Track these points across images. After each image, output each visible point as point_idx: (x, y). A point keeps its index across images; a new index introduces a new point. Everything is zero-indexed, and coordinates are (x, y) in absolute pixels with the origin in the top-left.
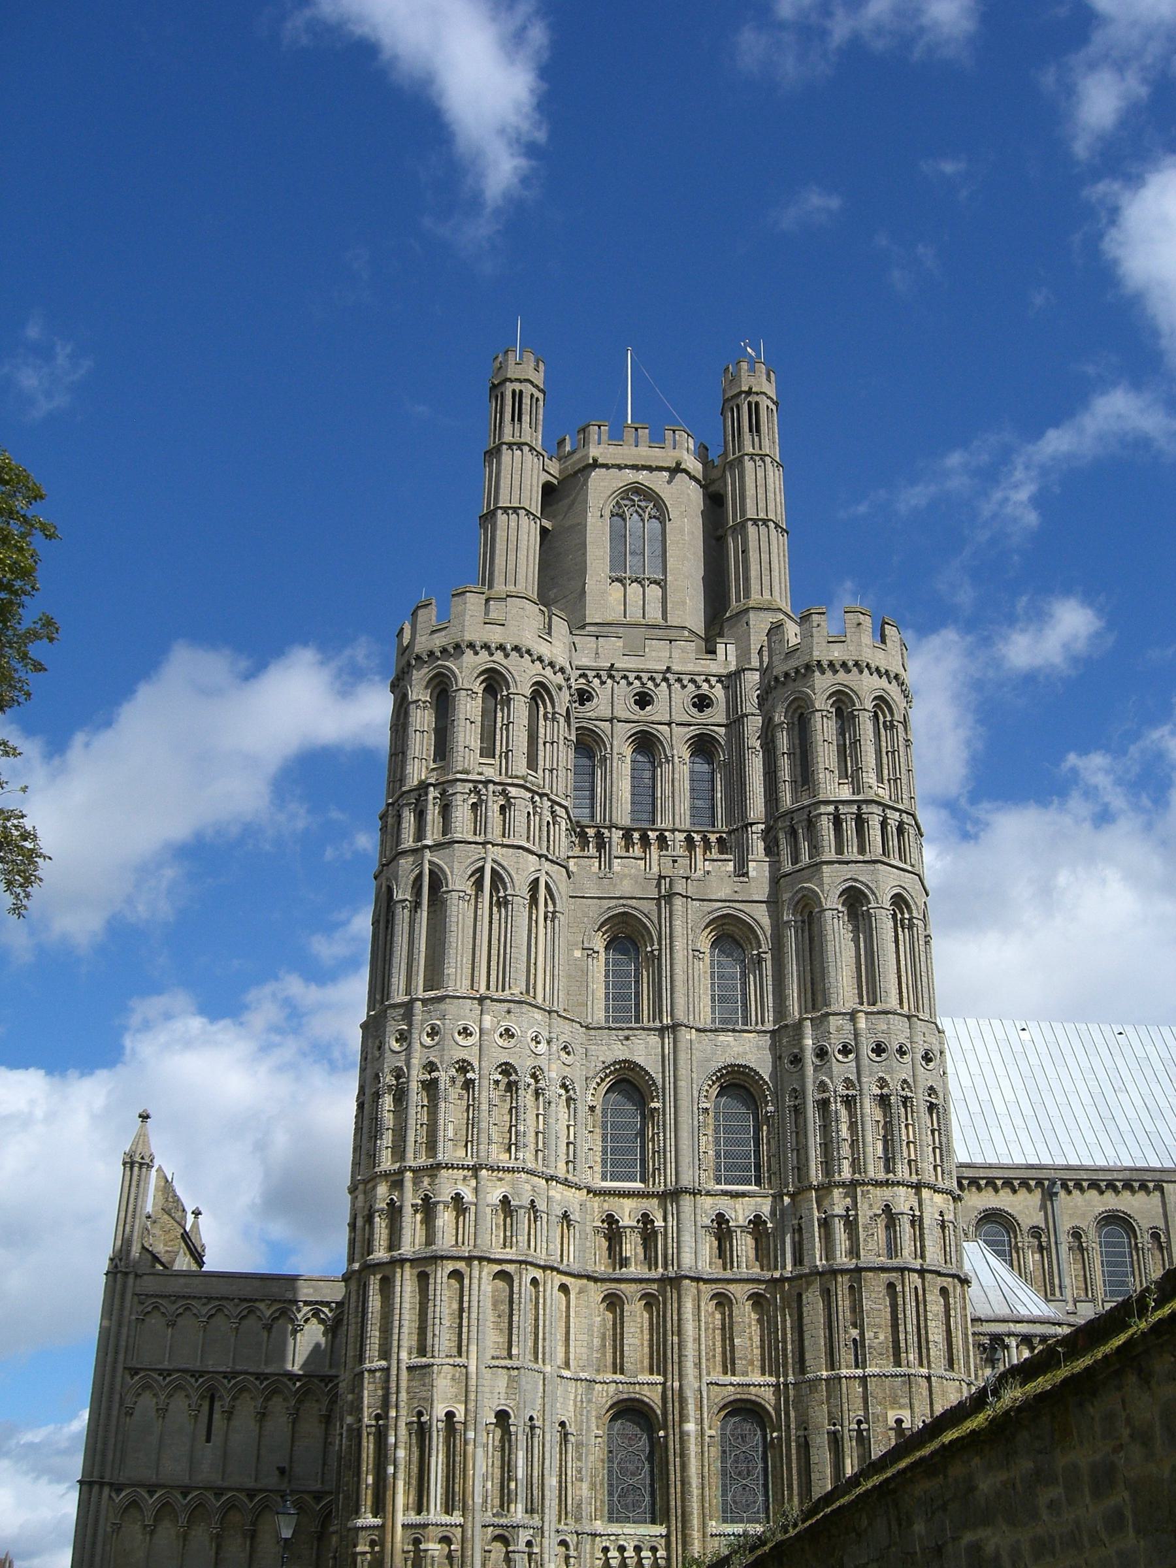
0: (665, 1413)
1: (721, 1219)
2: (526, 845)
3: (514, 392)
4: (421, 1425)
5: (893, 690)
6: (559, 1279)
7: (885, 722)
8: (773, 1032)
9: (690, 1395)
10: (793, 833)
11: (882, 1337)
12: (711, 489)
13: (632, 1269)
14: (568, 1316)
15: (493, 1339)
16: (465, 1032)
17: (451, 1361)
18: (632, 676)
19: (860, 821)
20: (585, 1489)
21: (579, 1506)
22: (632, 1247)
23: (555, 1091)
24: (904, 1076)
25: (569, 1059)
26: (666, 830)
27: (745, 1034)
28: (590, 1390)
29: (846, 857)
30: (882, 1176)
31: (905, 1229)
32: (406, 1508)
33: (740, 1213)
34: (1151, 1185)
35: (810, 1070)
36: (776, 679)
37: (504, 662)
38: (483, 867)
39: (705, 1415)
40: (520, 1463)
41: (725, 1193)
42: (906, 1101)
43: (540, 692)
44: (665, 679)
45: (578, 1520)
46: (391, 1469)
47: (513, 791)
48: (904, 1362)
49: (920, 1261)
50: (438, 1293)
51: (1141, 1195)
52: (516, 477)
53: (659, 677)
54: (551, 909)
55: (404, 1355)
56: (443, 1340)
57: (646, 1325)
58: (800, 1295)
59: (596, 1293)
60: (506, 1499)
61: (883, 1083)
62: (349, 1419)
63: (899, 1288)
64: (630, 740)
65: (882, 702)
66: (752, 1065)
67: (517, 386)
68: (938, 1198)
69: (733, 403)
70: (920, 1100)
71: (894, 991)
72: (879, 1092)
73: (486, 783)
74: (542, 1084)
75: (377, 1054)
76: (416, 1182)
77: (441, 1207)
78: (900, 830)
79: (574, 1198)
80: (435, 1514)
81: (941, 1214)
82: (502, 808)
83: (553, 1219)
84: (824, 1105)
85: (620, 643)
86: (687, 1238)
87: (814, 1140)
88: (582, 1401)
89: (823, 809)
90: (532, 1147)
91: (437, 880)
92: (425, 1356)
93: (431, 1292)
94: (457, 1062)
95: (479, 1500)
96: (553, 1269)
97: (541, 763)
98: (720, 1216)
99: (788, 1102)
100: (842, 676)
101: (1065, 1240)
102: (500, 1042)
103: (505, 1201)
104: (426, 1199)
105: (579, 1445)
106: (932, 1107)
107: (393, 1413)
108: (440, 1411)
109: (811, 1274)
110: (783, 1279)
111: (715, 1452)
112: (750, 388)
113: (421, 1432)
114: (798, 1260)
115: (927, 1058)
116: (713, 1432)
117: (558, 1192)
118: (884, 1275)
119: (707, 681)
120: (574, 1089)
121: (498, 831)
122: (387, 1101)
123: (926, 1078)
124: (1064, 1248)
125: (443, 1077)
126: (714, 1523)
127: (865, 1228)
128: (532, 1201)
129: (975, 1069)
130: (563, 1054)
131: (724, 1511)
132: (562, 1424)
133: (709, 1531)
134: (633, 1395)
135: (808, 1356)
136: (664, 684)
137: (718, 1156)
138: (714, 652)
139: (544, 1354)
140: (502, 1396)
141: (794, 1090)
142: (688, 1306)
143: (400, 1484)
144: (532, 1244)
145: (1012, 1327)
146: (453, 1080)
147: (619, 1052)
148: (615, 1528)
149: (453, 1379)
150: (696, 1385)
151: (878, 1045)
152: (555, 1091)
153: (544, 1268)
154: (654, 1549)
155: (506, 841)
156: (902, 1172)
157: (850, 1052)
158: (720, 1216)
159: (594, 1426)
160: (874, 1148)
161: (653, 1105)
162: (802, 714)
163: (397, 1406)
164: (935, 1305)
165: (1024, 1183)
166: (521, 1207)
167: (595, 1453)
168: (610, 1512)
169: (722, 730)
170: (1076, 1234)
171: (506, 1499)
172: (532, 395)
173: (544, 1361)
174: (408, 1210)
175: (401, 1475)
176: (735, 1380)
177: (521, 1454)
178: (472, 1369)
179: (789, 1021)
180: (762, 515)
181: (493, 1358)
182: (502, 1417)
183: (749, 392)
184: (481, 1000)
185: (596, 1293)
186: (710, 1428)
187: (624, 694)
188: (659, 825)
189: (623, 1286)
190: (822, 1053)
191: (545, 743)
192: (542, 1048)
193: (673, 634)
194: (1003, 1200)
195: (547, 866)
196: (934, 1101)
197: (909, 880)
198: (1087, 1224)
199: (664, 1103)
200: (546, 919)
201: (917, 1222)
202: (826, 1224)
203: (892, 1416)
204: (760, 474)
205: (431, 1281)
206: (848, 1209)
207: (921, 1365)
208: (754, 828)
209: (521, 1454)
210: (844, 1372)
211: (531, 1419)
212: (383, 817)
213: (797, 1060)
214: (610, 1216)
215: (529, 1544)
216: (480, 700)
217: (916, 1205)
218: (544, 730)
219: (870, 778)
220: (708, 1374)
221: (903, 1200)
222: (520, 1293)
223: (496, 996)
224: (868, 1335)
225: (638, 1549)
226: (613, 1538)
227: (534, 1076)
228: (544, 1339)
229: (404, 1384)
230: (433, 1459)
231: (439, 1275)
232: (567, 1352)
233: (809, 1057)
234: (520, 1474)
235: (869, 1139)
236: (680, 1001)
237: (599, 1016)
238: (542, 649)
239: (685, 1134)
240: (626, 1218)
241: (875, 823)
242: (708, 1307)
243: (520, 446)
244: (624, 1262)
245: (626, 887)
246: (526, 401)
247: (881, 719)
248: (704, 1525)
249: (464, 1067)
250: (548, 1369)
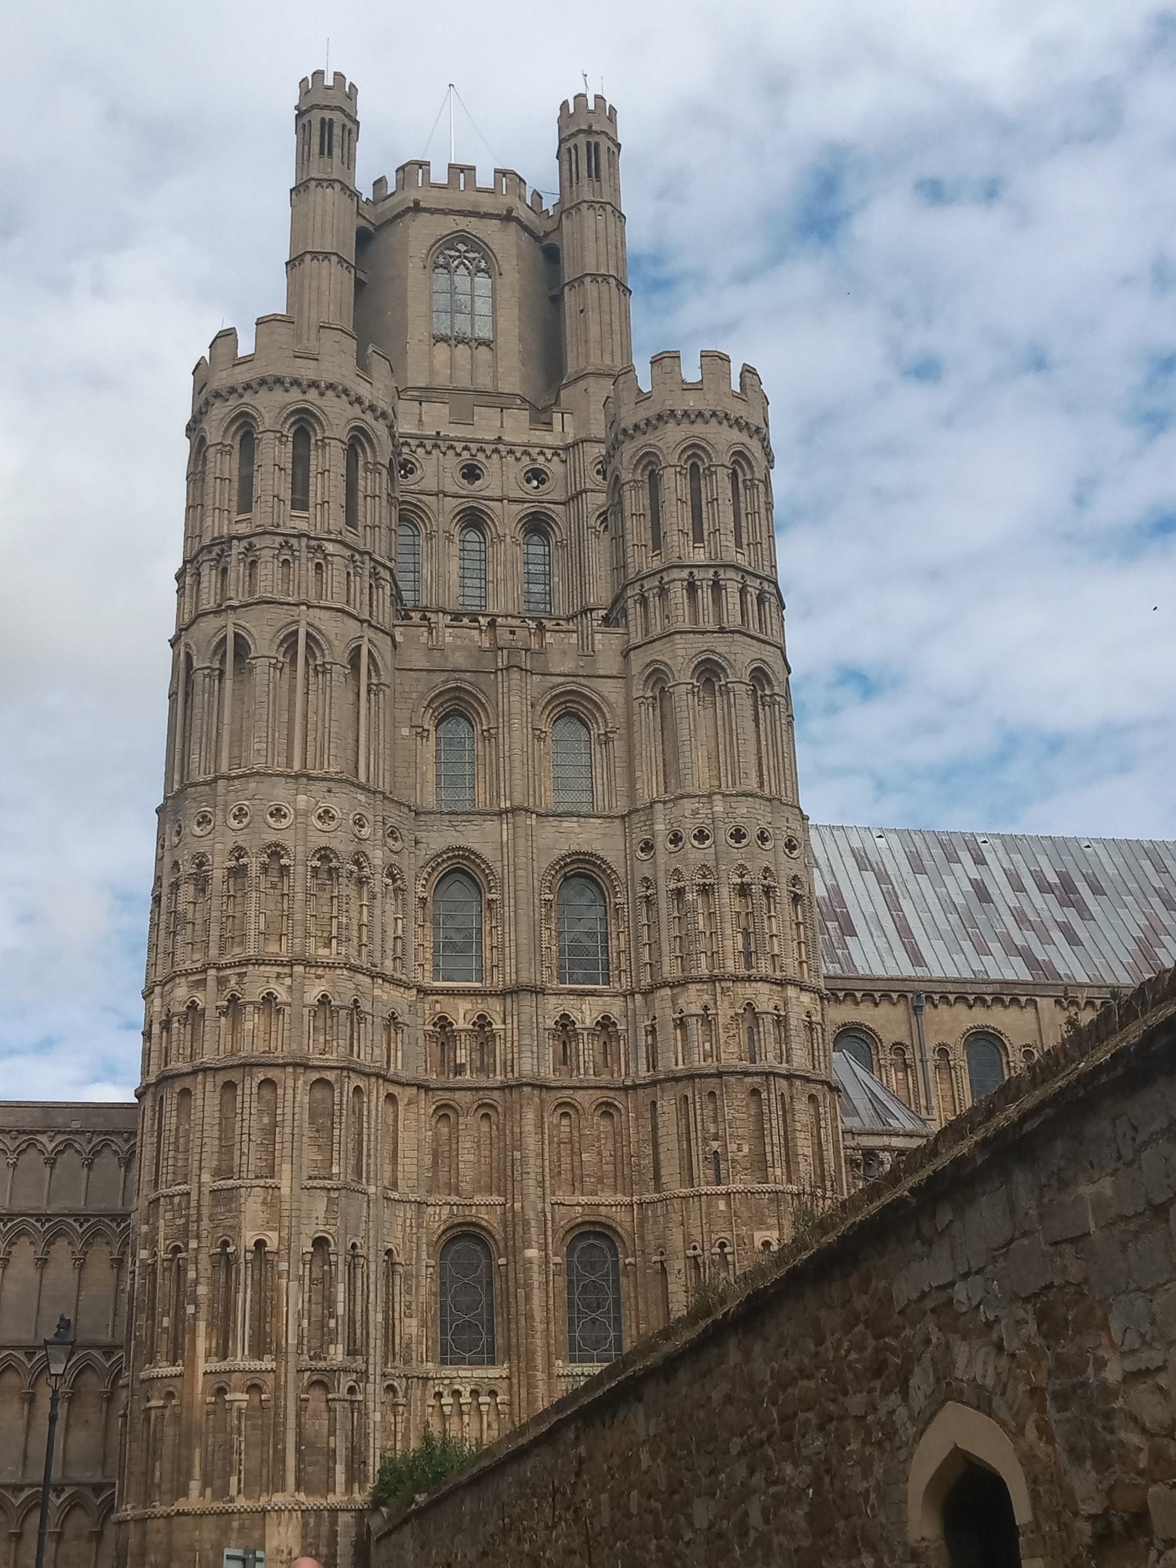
0: (505, 1239)
1: (565, 1022)
2: (347, 608)
3: (323, 119)
4: (224, 1254)
5: (755, 445)
6: (384, 1089)
7: (744, 481)
8: (623, 817)
9: (531, 1215)
10: (644, 601)
11: (746, 1149)
12: (546, 242)
13: (468, 1077)
14: (396, 1131)
15: (310, 1155)
16: (277, 813)
17: (261, 1182)
18: (459, 446)
19: (716, 586)
20: (411, 1327)
21: (408, 1346)
23: (379, 881)
24: (766, 864)
25: (398, 846)
26: (499, 616)
27: (592, 820)
28: (420, 1214)
29: (701, 626)
30: (742, 972)
31: (767, 1029)
32: (208, 1355)
33: (586, 1013)
34: (1023, 999)
35: (662, 858)
36: (625, 431)
37: (319, 401)
38: (296, 632)
39: (550, 1240)
40: (341, 1297)
41: (572, 992)
42: (768, 891)
43: (358, 440)
44: (496, 451)
45: (407, 1362)
46: (190, 1309)
47: (330, 548)
48: (771, 1178)
49: (785, 1065)
50: (247, 1105)
51: (1014, 1011)
53: (489, 448)
54: (374, 681)
55: (206, 1177)
56: (253, 1160)
57: (485, 1140)
58: (654, 1104)
59: (426, 1106)
61: (742, 870)
62: (144, 1254)
63: (764, 1095)
64: (458, 517)
65: (741, 456)
66: (601, 853)
67: (328, 115)
68: (806, 998)
69: (570, 144)
70: (783, 893)
71: (754, 774)
72: (739, 881)
73: (299, 536)
74: (367, 872)
75: (176, 840)
76: (221, 982)
77: (250, 1008)
78: (761, 600)
79: (400, 999)
80: (241, 1360)
81: (809, 1015)
82: (318, 566)
83: (378, 1020)
84: (680, 893)
85: (446, 410)
87: (667, 933)
88: (411, 1226)
89: (676, 574)
90: (356, 940)
91: (241, 647)
92: (231, 1178)
93: (239, 1105)
94: (269, 847)
95: (292, 1341)
96: (378, 1076)
97: (361, 518)
98: (565, 1016)
99: (641, 891)
100: (699, 428)
101: (931, 1057)
102: (319, 825)
103: (324, 1001)
104: (233, 999)
105: (407, 1276)
106: (796, 899)
107: (193, 1244)
109: (666, 1080)
110: (635, 1087)
111: (562, 1282)
112: (591, 127)
114: (653, 1064)
115: (790, 846)
116: (558, 1260)
117: (384, 993)
118: (748, 1080)
119: (542, 453)
120: (402, 879)
121: (312, 592)
123: (787, 867)
124: (930, 1066)
125: (253, 864)
126: (560, 1362)
127: (726, 1029)
128: (356, 1001)
130: (390, 841)
131: (572, 1349)
132: (389, 1252)
133: (555, 1371)
134: (469, 1218)
135: (663, 1172)
136: (495, 456)
137: (561, 951)
138: (550, 424)
139: (368, 1173)
140: (321, 1220)
141: (646, 879)
142: (530, 1116)
143: (202, 1326)
144: (355, 1049)
145: (885, 1141)
146: (265, 869)
148: (449, 1371)
149: (264, 1203)
150: (540, 1207)
151: (738, 830)
152: (379, 881)
153: (368, 1075)
154: (493, 1393)
155: (323, 603)
156: (764, 967)
157: (707, 837)
158: (565, 1016)
159: (424, 1255)
160: (733, 943)
161: (490, 896)
162: (653, 471)
163: (198, 1237)
164: (803, 1114)
165: (886, 996)
166: (342, 1008)
167: (426, 1286)
168: (444, 1352)
169: (560, 509)
170: (943, 1051)
172: (344, 126)
173: (368, 1181)
175: (203, 1314)
176: (584, 1199)
177: (341, 1287)
178: (285, 1191)
179: (639, 805)
180: (602, 271)
181: (310, 1178)
182: (320, 1243)
183: (589, 131)
184: (297, 777)
185: (426, 1106)
186: (556, 1255)
187: (452, 464)
188: (491, 609)
189: (458, 1095)
190: (676, 839)
191: (366, 497)
192: (366, 832)
193: (505, 401)
194: (865, 1014)
195: (369, 633)
196: (798, 891)
197: (769, 654)
198: (955, 1041)
199: (502, 894)
200: (369, 691)
201: (781, 1022)
202: (681, 1024)
203: (759, 1237)
204: (601, 225)
205: (239, 1092)
206: (706, 1008)
207: (790, 1181)
208: (594, 614)
209: (341, 1287)
210: (705, 1189)
211: (354, 1246)
212: (179, 577)
213: (648, 847)
214: (444, 1018)
215: (351, 1390)
216: (290, 445)
217: (781, 1003)
218: (364, 483)
220: (553, 1194)
221: (764, 997)
222: (341, 1104)
223: (314, 773)
224: (733, 1147)
225: (475, 1393)
226: (447, 1382)
227: (357, 863)
228: (369, 1156)
229: (205, 1211)
230: (240, 1296)
231: (247, 1085)
232: (394, 1171)
233: (662, 844)
234: (340, 1309)
235: (728, 931)
238: (363, 390)
239: (523, 927)
240: (461, 1021)
241: (733, 589)
242: (552, 1119)
243: (331, 182)
246: (337, 131)
247: (740, 479)
248: (550, 1365)
249: (275, 851)
250: (372, 1189)
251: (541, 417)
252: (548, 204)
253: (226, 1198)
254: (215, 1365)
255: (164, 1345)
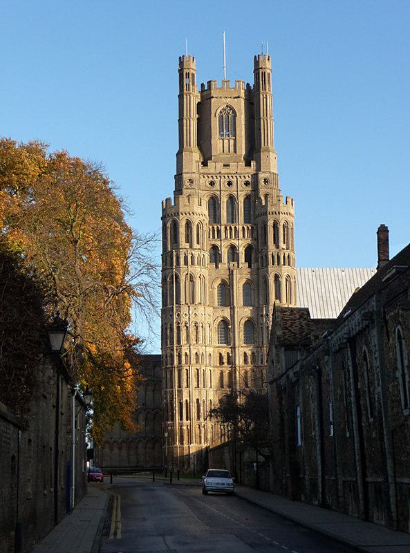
15: (194, 383)
22: (225, 360)
52: (188, 106)
56: (184, 384)
60: (199, 418)
86: (237, 358)
108: (184, 399)
113: (181, 404)
122: (168, 331)
129: (327, 286)
138: (250, 165)
147: (221, 314)
171: (199, 418)
174: (175, 356)
182: (198, 400)
213: (262, 316)
219: (282, 245)
236: (235, 301)
237: (216, 304)
244: (223, 363)
245: (222, 272)
251: (248, 164)
252: (252, 84)
253: (180, 392)
254: (180, 422)
255: (170, 417)
